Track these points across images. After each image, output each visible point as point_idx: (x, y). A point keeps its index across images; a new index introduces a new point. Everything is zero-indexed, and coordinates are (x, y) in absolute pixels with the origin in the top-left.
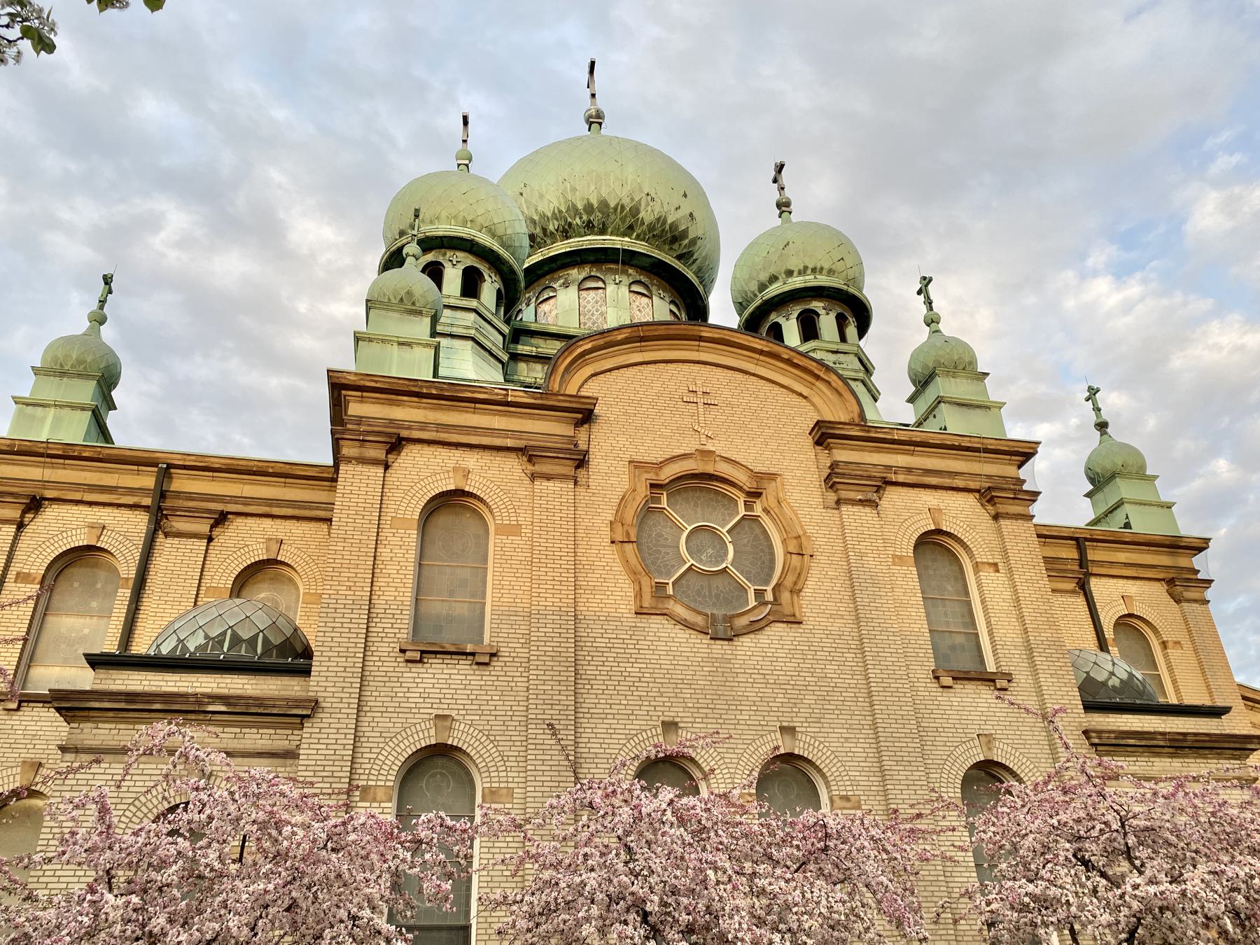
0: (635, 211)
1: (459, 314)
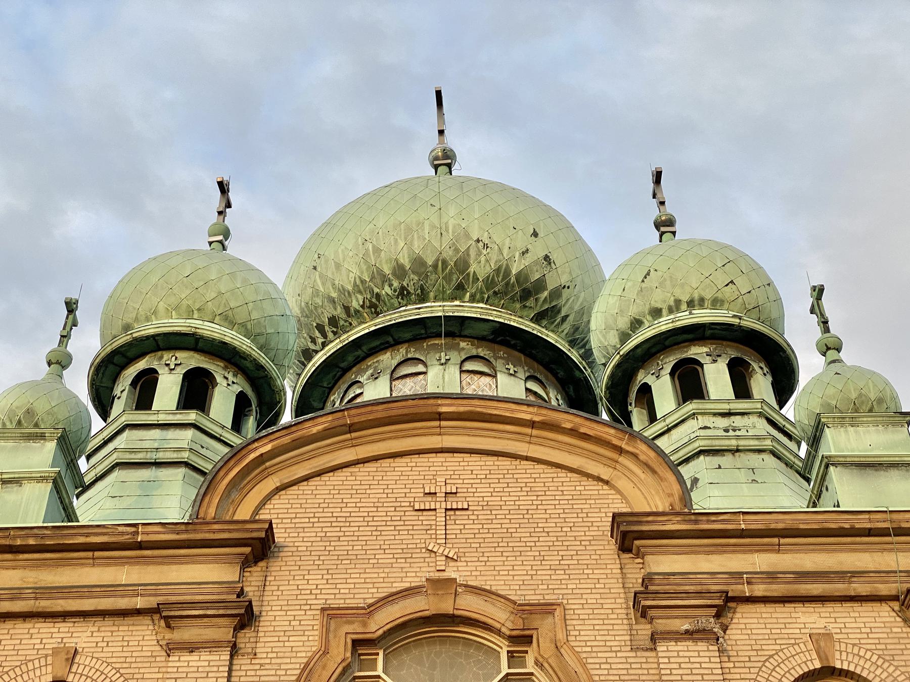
0: (462, 265)
1: (171, 434)
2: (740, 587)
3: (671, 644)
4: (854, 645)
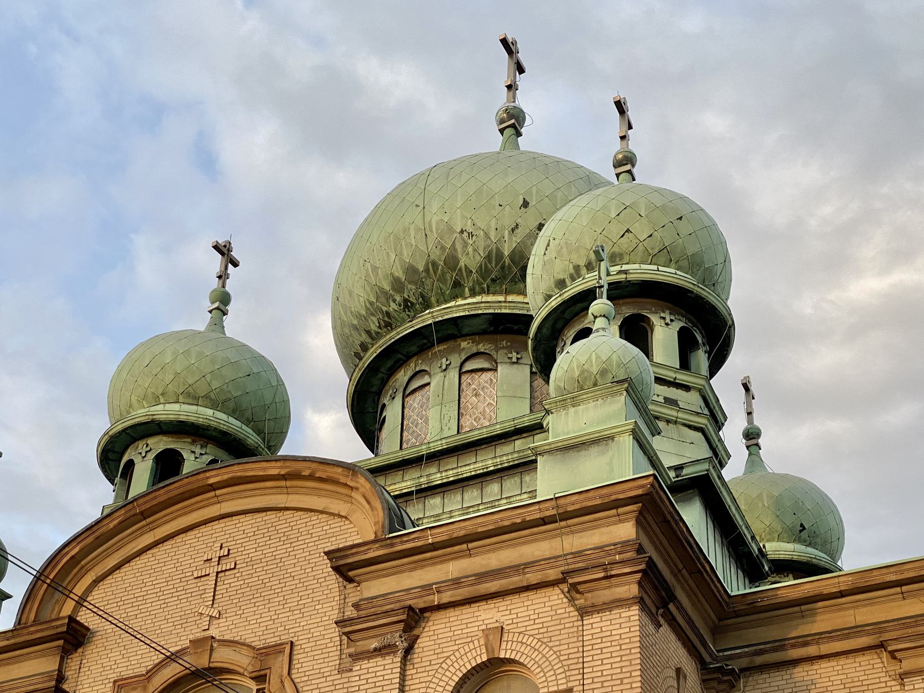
0: (452, 262)
2: (431, 597)
3: (364, 662)
4: (520, 633)
